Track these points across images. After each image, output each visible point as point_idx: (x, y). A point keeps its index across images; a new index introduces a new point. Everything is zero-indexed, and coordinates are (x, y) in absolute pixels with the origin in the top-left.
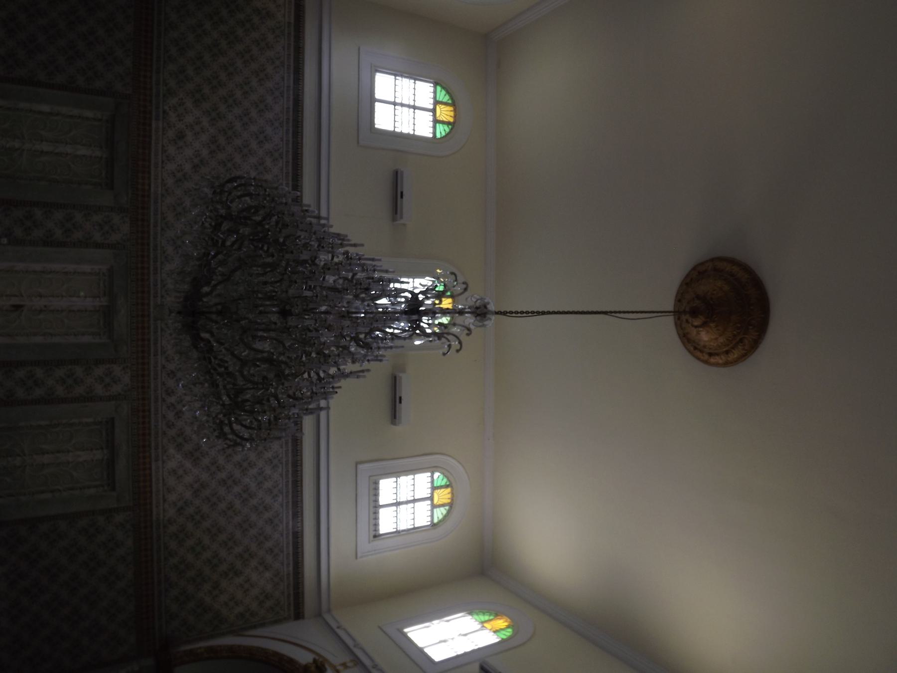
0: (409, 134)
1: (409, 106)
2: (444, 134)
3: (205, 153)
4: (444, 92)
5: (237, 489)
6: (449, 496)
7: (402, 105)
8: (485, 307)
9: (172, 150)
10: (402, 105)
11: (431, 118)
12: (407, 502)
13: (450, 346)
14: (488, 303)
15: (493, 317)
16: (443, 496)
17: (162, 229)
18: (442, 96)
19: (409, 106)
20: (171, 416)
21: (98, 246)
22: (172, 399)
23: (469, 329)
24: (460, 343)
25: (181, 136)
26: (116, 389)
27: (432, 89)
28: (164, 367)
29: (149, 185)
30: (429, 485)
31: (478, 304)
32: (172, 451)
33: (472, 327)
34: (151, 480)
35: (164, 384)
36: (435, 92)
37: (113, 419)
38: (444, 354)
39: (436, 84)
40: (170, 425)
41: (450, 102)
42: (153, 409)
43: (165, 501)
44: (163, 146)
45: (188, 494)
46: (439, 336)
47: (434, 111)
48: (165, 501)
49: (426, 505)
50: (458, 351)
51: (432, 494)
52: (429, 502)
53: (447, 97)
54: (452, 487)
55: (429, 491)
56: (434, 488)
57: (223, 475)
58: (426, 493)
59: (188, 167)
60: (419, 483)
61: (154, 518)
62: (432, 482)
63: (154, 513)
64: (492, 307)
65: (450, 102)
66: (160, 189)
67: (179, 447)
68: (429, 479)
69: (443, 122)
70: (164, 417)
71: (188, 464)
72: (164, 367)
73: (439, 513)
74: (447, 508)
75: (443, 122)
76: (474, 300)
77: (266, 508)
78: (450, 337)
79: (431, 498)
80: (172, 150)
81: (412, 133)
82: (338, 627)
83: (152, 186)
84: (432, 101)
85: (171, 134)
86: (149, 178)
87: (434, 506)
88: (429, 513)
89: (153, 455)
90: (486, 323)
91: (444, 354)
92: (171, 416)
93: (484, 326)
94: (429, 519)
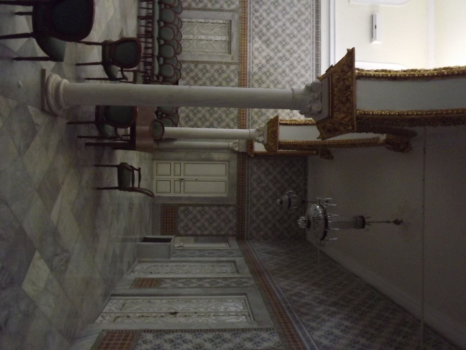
5: (287, 63)
32: (257, 39)
34: (247, 51)
37: (231, 21)
42: (248, 18)
43: (253, 63)
45: (264, 62)
48: (253, 63)
57: (280, 55)
61: (248, 70)
63: (248, 68)
67: (260, 38)
70: (253, 22)
71: (264, 47)
77: (302, 76)
89: (248, 40)
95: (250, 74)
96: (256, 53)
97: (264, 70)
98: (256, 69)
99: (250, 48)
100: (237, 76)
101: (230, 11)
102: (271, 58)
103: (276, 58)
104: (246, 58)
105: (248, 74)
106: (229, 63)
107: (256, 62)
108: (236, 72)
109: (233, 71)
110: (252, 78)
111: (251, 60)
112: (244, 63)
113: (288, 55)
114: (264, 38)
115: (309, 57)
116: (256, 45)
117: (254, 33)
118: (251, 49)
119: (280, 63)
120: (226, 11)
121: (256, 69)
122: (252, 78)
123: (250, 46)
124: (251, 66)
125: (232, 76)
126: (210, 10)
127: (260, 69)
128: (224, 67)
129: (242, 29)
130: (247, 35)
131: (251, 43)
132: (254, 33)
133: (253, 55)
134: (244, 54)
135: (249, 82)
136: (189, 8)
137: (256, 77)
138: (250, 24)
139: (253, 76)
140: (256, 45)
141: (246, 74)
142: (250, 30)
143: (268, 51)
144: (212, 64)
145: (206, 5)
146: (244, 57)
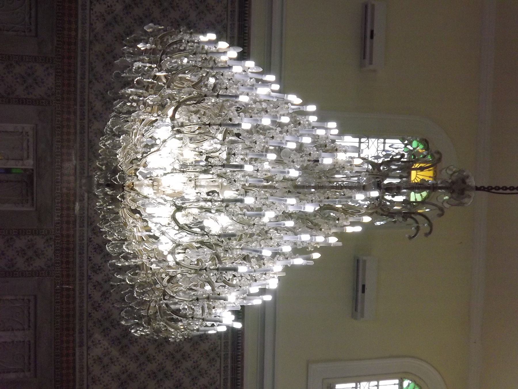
8: (463, 181)
13: (418, 228)
14: (468, 177)
15: (473, 194)
17: (90, 82)
20: (97, 296)
21: (21, 101)
22: (99, 277)
23: (442, 209)
24: (431, 225)
26: (39, 263)
28: (90, 240)
29: (76, 30)
31: (454, 178)
32: (97, 336)
33: (446, 205)
35: (90, 259)
37: (35, 297)
38: (410, 238)
40: (96, 307)
46: (406, 216)
50: (427, 235)
57: (152, 367)
64: (472, 182)
66: (87, 35)
67: (105, 332)
70: (90, 297)
71: (115, 353)
72: (90, 240)
76: (450, 172)
78: (418, 218)
83: (80, 31)
86: (76, 22)
89: (77, 340)
90: (466, 200)
91: (410, 238)
92: (97, 296)
93: (461, 204)
96: (96, 370)
114: (115, 333)
115: (218, 365)
116: (97, 351)
118: (85, 360)
130: (74, 329)
131: (85, 348)
133: (89, 373)
140: (97, 351)
142: (81, 315)
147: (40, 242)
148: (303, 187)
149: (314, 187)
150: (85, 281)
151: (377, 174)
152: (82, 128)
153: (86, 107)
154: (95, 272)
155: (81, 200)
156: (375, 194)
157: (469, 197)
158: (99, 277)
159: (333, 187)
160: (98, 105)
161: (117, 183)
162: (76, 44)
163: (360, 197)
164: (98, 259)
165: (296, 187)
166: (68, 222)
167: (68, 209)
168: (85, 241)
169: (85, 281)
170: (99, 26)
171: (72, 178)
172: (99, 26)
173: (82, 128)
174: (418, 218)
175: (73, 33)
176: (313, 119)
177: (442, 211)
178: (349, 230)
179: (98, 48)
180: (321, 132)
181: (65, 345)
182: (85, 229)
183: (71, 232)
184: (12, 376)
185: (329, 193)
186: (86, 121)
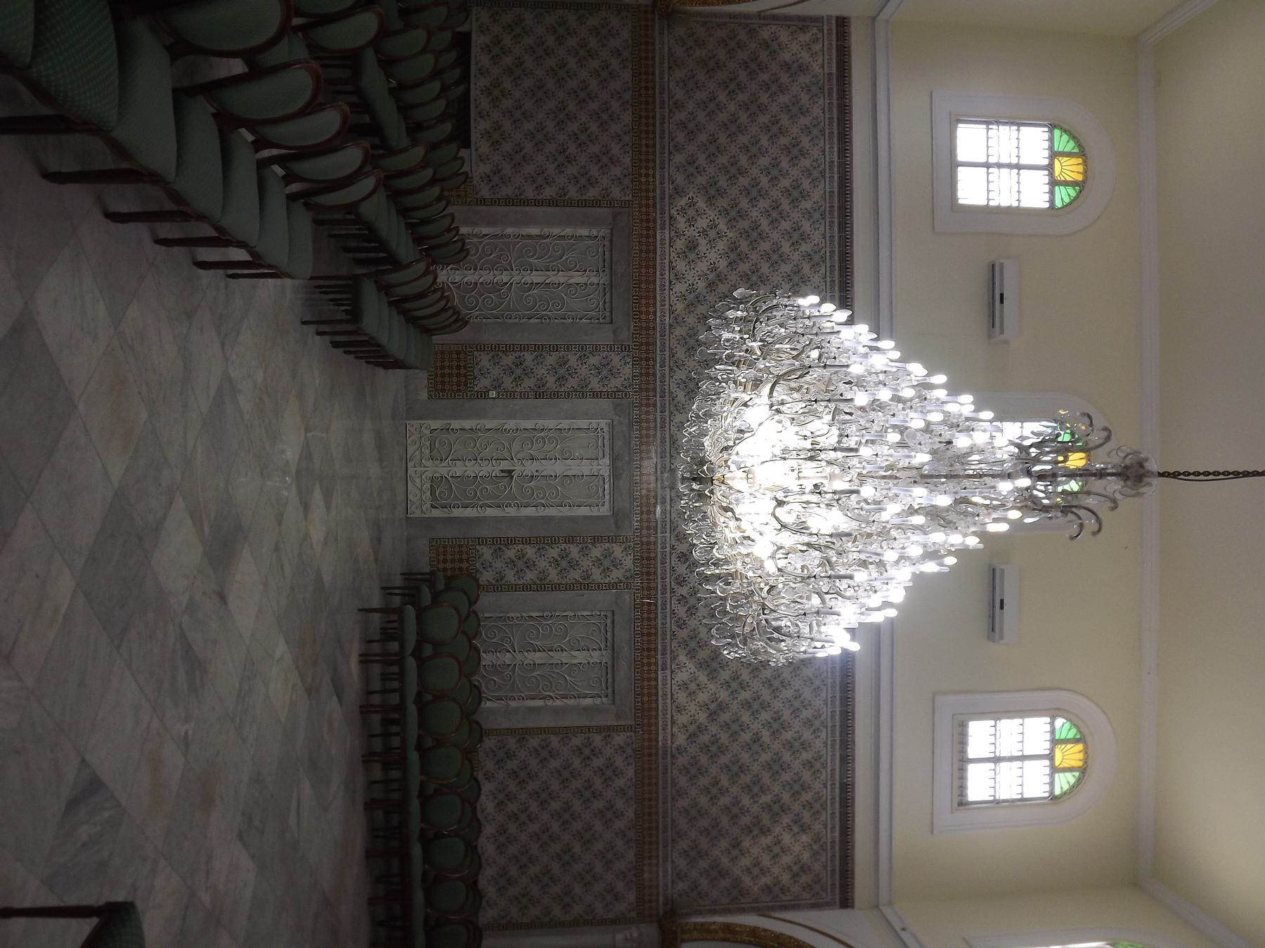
0: (1009, 208)
1: (1010, 166)
2: (1067, 200)
3: (723, 264)
4: (1065, 137)
6: (1081, 756)
7: (999, 166)
8: (1141, 465)
9: (681, 266)
10: (999, 166)
11: (1046, 179)
12: (1012, 759)
13: (1081, 526)
15: (1156, 481)
16: (1071, 755)
18: (1063, 142)
19: (1010, 166)
20: (681, 611)
21: (596, 395)
22: (684, 591)
23: (1114, 501)
25: (692, 246)
26: (616, 574)
27: (1046, 136)
28: (673, 548)
30: (1048, 736)
31: (1128, 462)
32: (682, 658)
33: (1118, 496)
35: (673, 570)
36: (1051, 140)
38: (1072, 538)
39: (1052, 127)
40: (682, 625)
41: (1076, 150)
43: (673, 723)
44: (670, 262)
45: (702, 717)
46: (1066, 510)
47: (1050, 168)
48: (673, 723)
49: (1042, 767)
51: (1052, 750)
52: (1047, 762)
53: (1072, 144)
54: (1085, 743)
55: (1048, 745)
56: (1055, 742)
57: (746, 695)
58: (1044, 748)
59: (701, 285)
60: (1034, 732)
62: (1053, 732)
63: (660, 738)
64: (1153, 466)
65: (1076, 150)
67: (692, 654)
68: (1048, 728)
69: (1066, 183)
70: (673, 612)
71: (703, 678)
72: (673, 548)
73: (1064, 782)
74: (1077, 774)
75: (1066, 183)
76: (1123, 455)
77: (805, 746)
78: (1082, 513)
79: (1051, 757)
80: (681, 266)
81: (1015, 204)
82: (903, 929)
84: (1046, 153)
85: (680, 244)
87: (1054, 770)
88: (1047, 779)
91: (1072, 538)
92: (681, 611)
93: (1139, 495)
94: (1047, 788)
95: (665, 753)
96: (682, 697)
97: (705, 738)
98: (681, 739)
99: (664, 685)
100: (631, 761)
101: (611, 586)
102: (722, 707)
103: (735, 706)
104: (653, 713)
105: (660, 752)
106: (609, 728)
107: (682, 719)
108: (629, 751)
109: (621, 749)
110: (673, 764)
111: (669, 716)
112: (650, 725)
113: (766, 694)
114: (702, 654)
116: (682, 676)
117: (675, 644)
119: (746, 717)
120: (599, 586)
121: (681, 739)
122: (673, 764)
123: (665, 678)
124: (669, 731)
125: (619, 762)
126: (556, 587)
127: (692, 737)
128: (597, 739)
129: (643, 635)
131: (668, 672)
132: (675, 644)
133: (673, 701)
134: (649, 702)
135: (665, 773)
136: (499, 586)
137: (682, 760)
138: (664, 618)
139: (673, 756)
140: (682, 676)
141: (657, 754)
142: (664, 633)
143: (712, 687)
144: (565, 733)
145: (543, 575)
146: (650, 710)
147: (618, 550)
148: (931, 476)
149: (946, 477)
150: (668, 595)
151: (1024, 460)
152: (663, 421)
153: (667, 398)
154: (679, 584)
155: (663, 503)
156: (1025, 482)
157: (1150, 485)
158: (684, 591)
159: (969, 476)
160: (681, 396)
161: (703, 477)
162: (654, 328)
163: (1005, 487)
164: (682, 569)
165: (923, 476)
166: (648, 528)
167: (649, 512)
168: (668, 549)
169: (668, 595)
170: (680, 307)
171: (652, 478)
172: (680, 307)
173: (663, 421)
174: (1082, 513)
175: (651, 317)
176: (941, 394)
177: (1115, 505)
178: (993, 528)
179: (679, 331)
180: (952, 408)
181: (646, 668)
182: (668, 534)
183: (652, 539)
184: (588, 701)
185: (966, 482)
186: (667, 413)
